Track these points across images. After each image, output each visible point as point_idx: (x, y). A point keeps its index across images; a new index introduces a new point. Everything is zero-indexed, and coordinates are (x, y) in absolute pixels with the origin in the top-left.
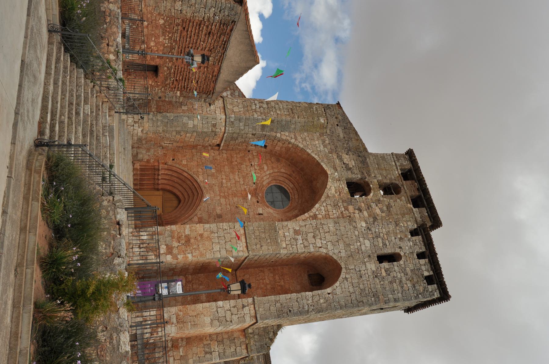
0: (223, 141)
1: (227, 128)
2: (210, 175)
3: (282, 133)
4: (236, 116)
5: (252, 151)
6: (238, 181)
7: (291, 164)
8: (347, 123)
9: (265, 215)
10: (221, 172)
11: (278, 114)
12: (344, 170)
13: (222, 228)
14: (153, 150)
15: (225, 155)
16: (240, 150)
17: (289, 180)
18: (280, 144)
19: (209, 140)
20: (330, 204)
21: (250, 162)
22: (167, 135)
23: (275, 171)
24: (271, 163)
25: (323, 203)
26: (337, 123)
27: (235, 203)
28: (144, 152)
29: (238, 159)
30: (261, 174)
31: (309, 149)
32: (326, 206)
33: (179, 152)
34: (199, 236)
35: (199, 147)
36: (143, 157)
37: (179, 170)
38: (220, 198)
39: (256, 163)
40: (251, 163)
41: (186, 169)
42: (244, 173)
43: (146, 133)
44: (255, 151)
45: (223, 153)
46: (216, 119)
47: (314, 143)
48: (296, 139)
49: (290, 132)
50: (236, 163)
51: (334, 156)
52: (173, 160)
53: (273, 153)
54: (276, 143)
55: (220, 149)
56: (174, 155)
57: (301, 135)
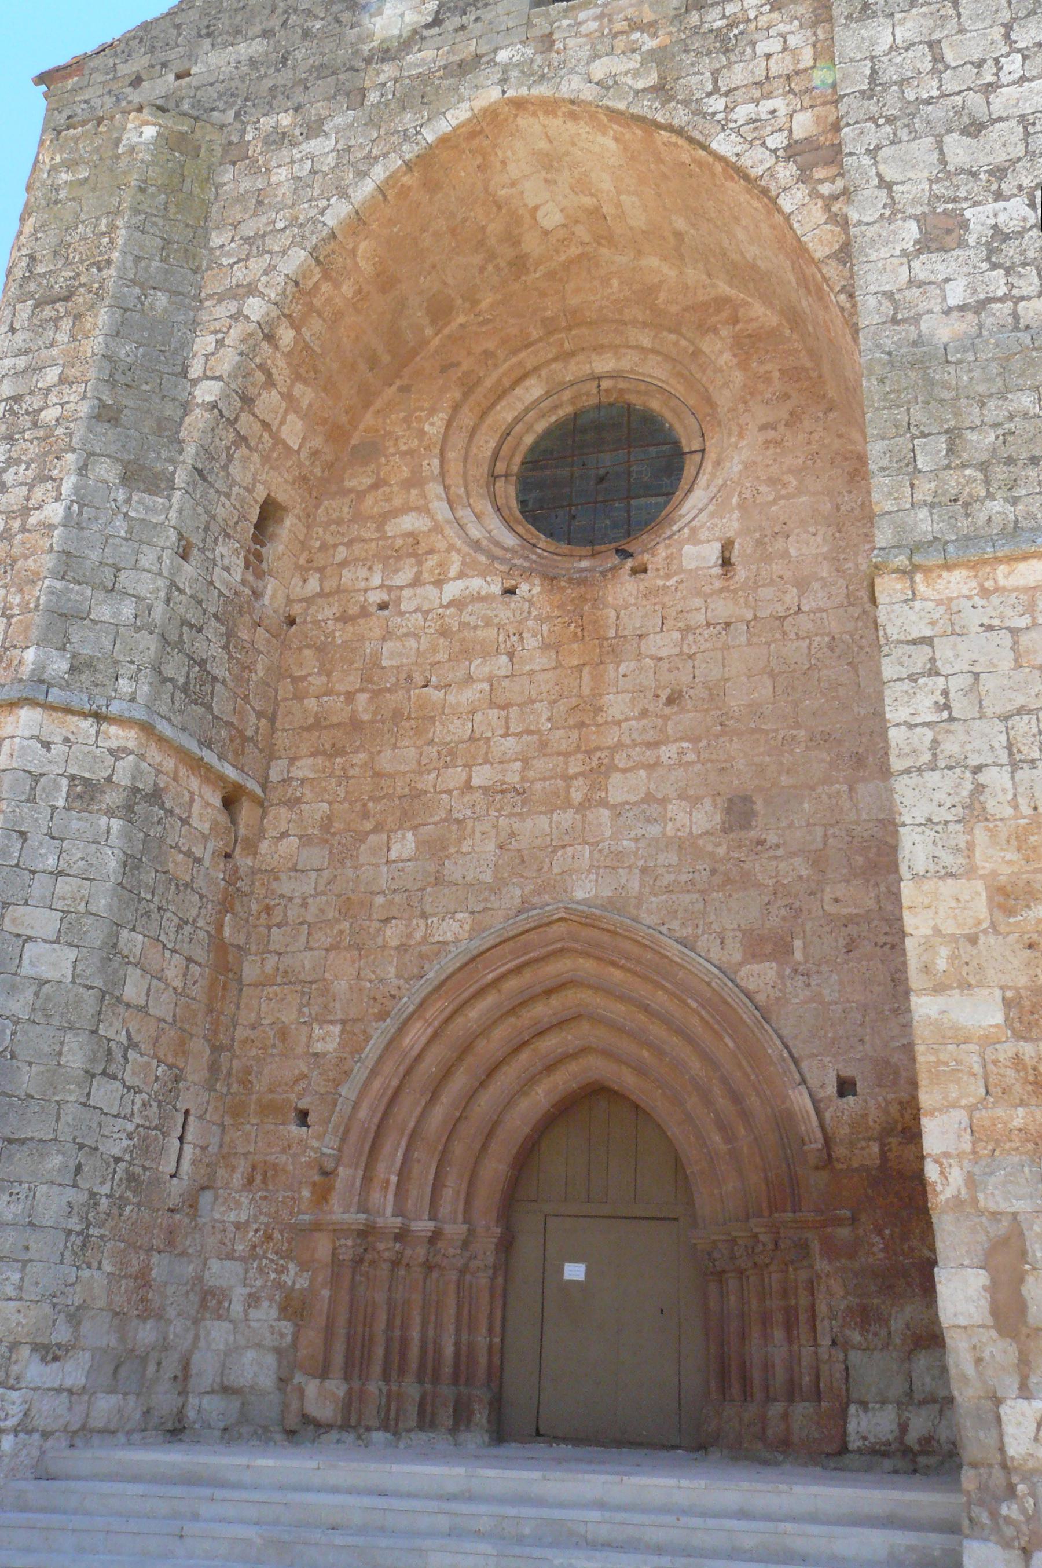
0: (210, 757)
1: (115, 708)
2: (432, 868)
3: (195, 372)
4: (34, 634)
5: (289, 601)
6: (486, 686)
7: (398, 383)
8: (178, 27)
9: (732, 524)
10: (418, 794)
11: (63, 380)
12: (477, 20)
13: (929, 734)
14: (215, 1265)
15: (304, 769)
16: (279, 672)
17: (500, 398)
18: (269, 401)
19: (188, 854)
20: (715, 75)
21: (364, 612)
22: (116, 1151)
23: (436, 471)
24: (387, 489)
25: (704, 115)
26: (171, 77)
27: (644, 713)
28: (218, 1333)
29: (339, 687)
30: (452, 547)
31: (322, 213)
32: (727, 94)
33: (248, 1070)
34: (1010, 912)
35: (227, 932)
36: (259, 1346)
37: (377, 1084)
38: (604, 803)
39: (376, 580)
40: (373, 609)
41: (379, 1033)
42: (435, 650)
43: (75, 1317)
44: (296, 581)
45: (286, 781)
46: (36, 778)
47: (285, 190)
48: (251, 289)
49: (194, 325)
50: (362, 698)
51: (382, 78)
52: (303, 1118)
53: (318, 471)
54: (257, 426)
55: (258, 791)
56: (269, 1109)
57: (225, 261)
